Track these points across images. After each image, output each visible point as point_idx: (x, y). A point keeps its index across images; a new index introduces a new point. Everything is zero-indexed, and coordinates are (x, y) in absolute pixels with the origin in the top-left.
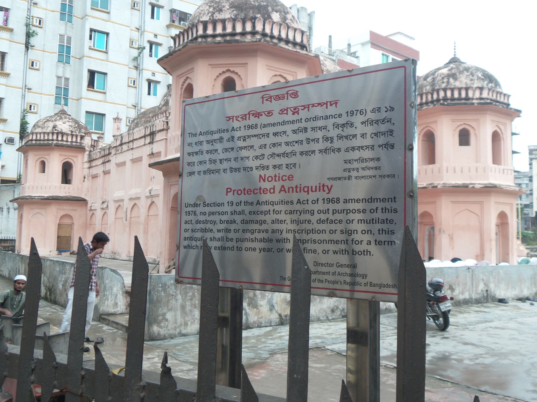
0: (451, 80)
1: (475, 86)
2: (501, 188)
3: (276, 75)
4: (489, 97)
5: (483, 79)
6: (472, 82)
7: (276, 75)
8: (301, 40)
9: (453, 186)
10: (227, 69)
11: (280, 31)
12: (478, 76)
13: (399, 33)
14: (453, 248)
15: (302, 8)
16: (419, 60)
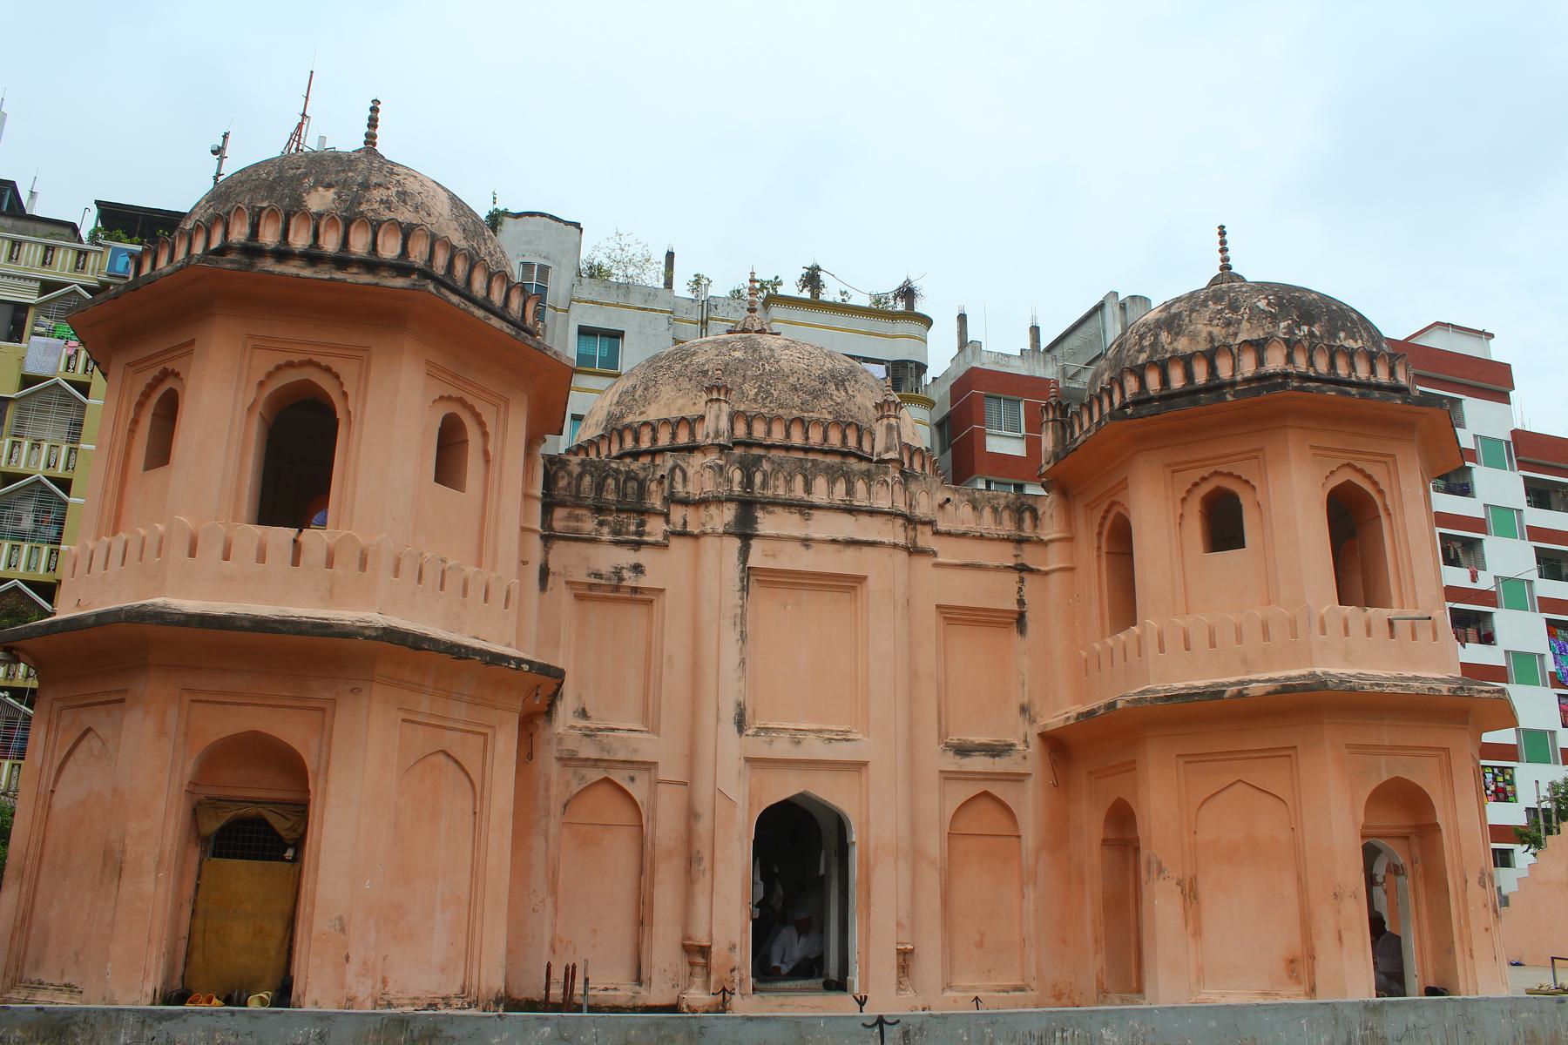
0: (1164, 337)
1: (1242, 337)
2: (1352, 689)
3: (290, 365)
4: (1290, 369)
5: (1273, 317)
6: (1231, 330)
7: (290, 365)
8: (398, 251)
9: (1168, 698)
10: (160, 368)
11: (316, 235)
12: (1253, 309)
13: (1437, 323)
14: (1197, 933)
15: (1133, 297)
16: (1513, 388)
